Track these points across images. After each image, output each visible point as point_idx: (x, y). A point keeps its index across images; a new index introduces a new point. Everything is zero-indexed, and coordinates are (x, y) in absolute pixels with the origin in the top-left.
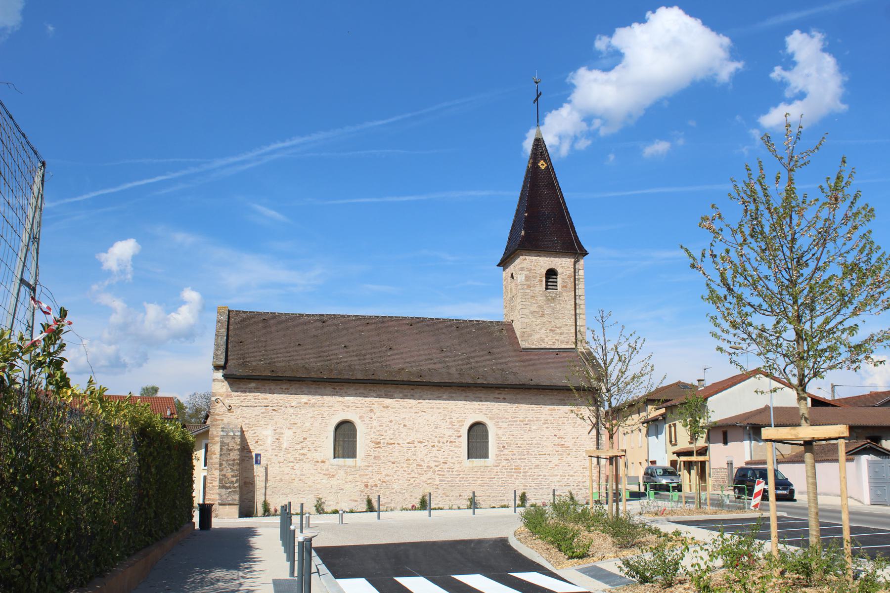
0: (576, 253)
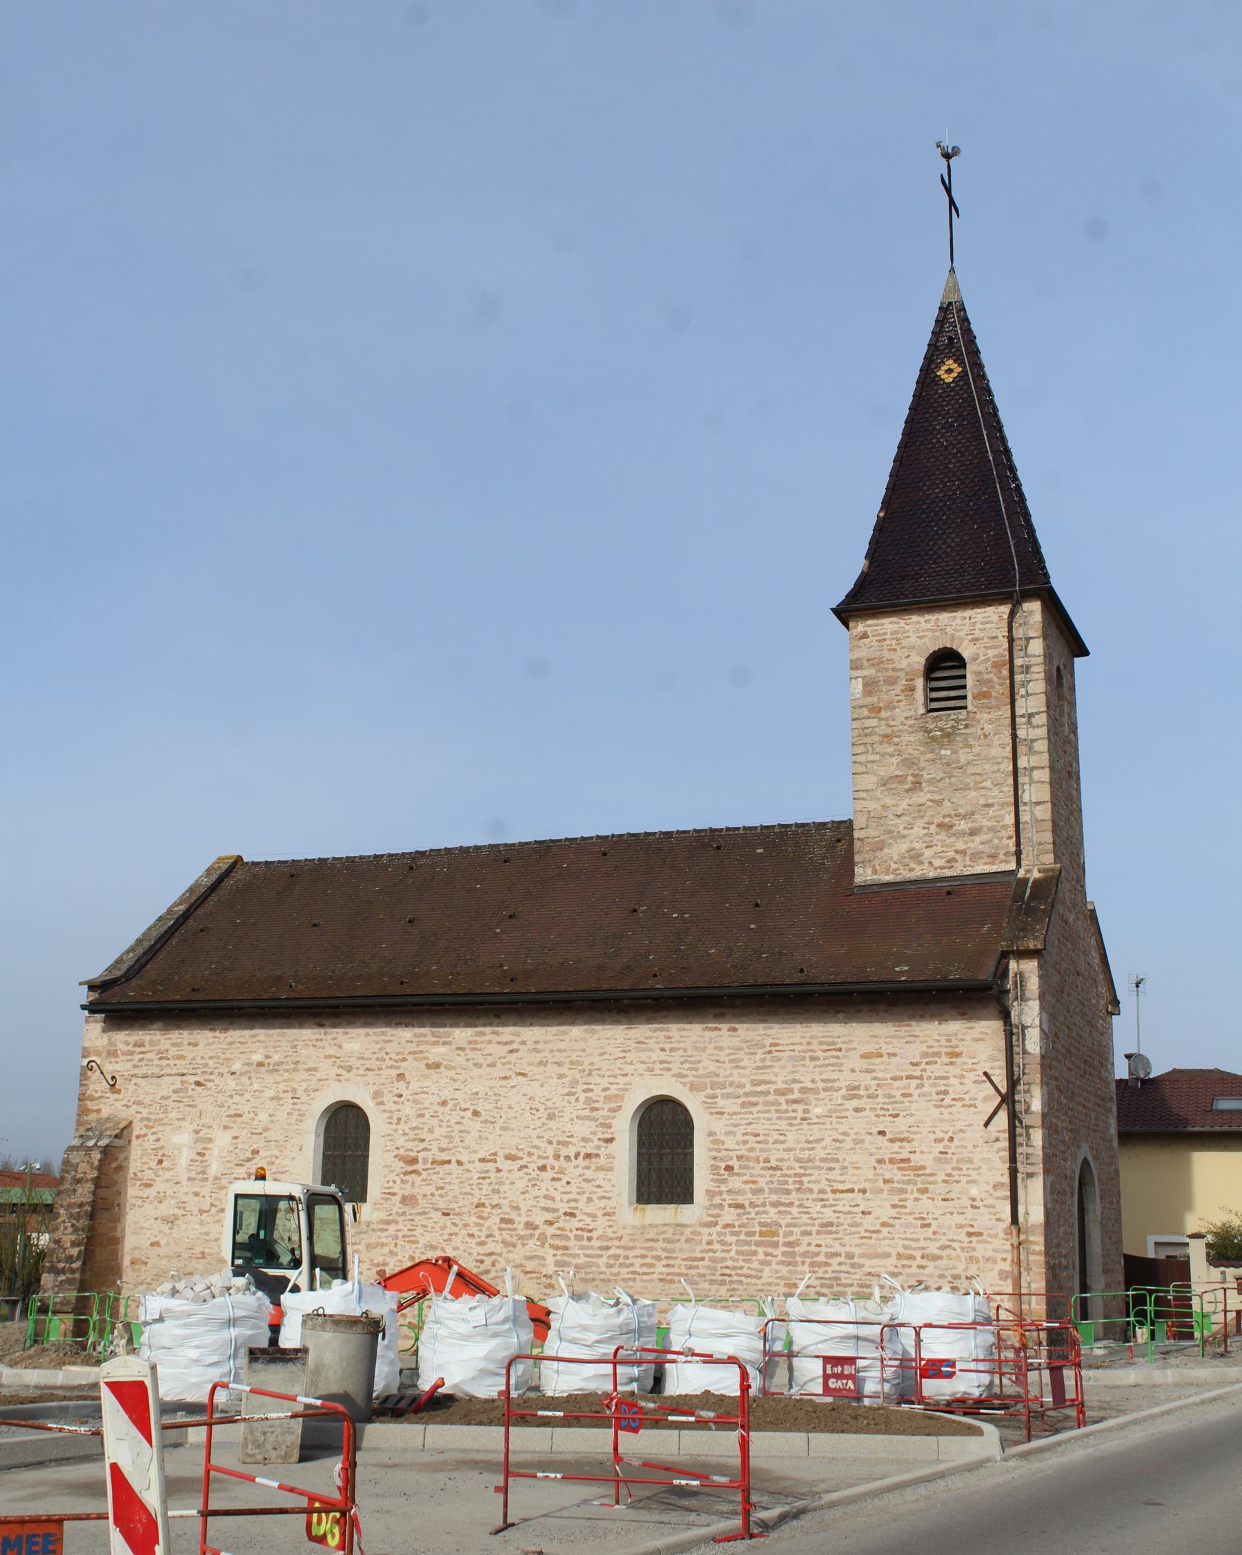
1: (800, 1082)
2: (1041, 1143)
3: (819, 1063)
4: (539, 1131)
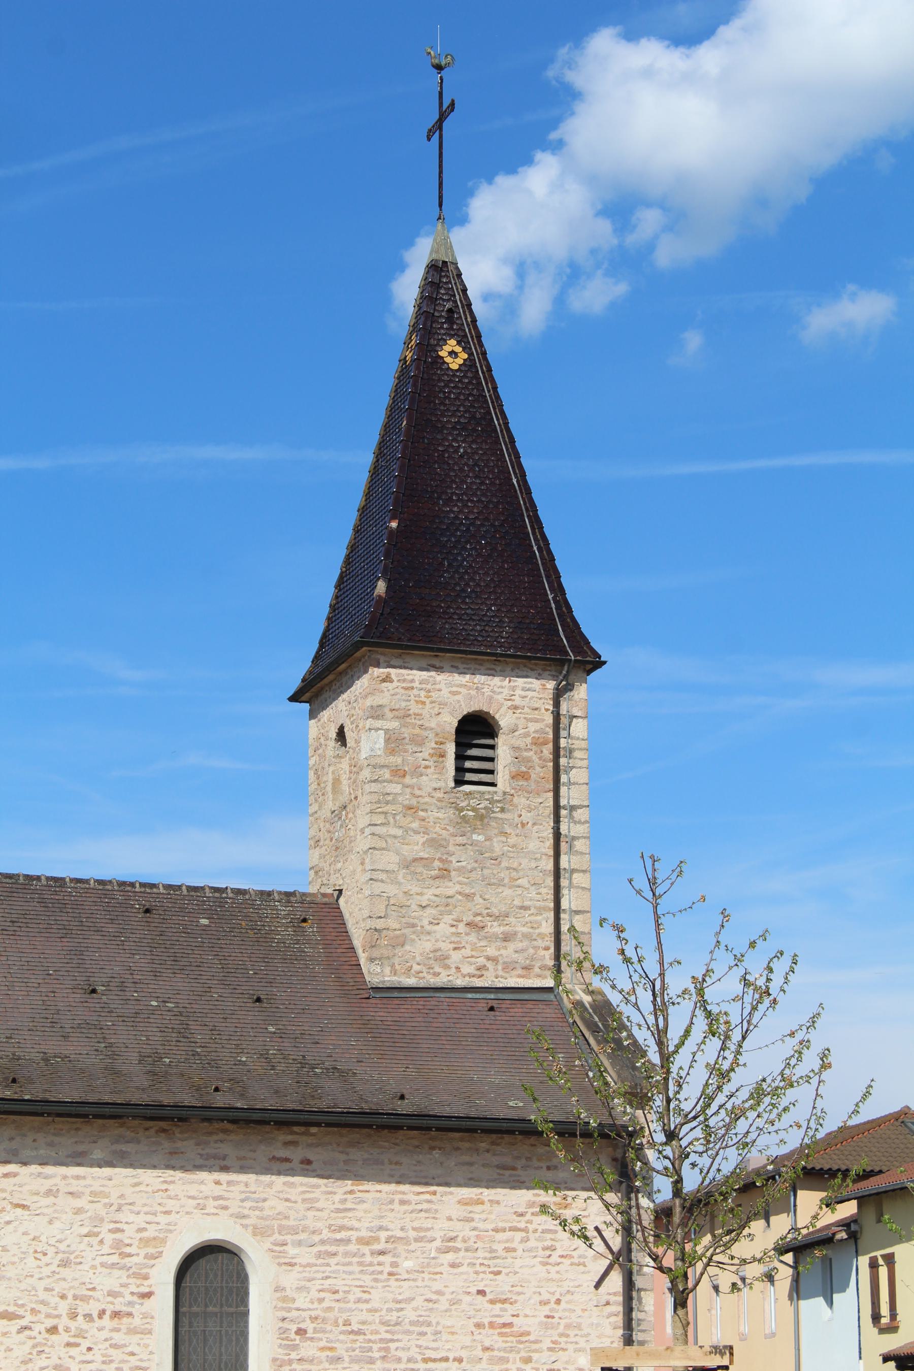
0: (561, 663)
1: (387, 1230)
3: (410, 1208)
4: (46, 1282)
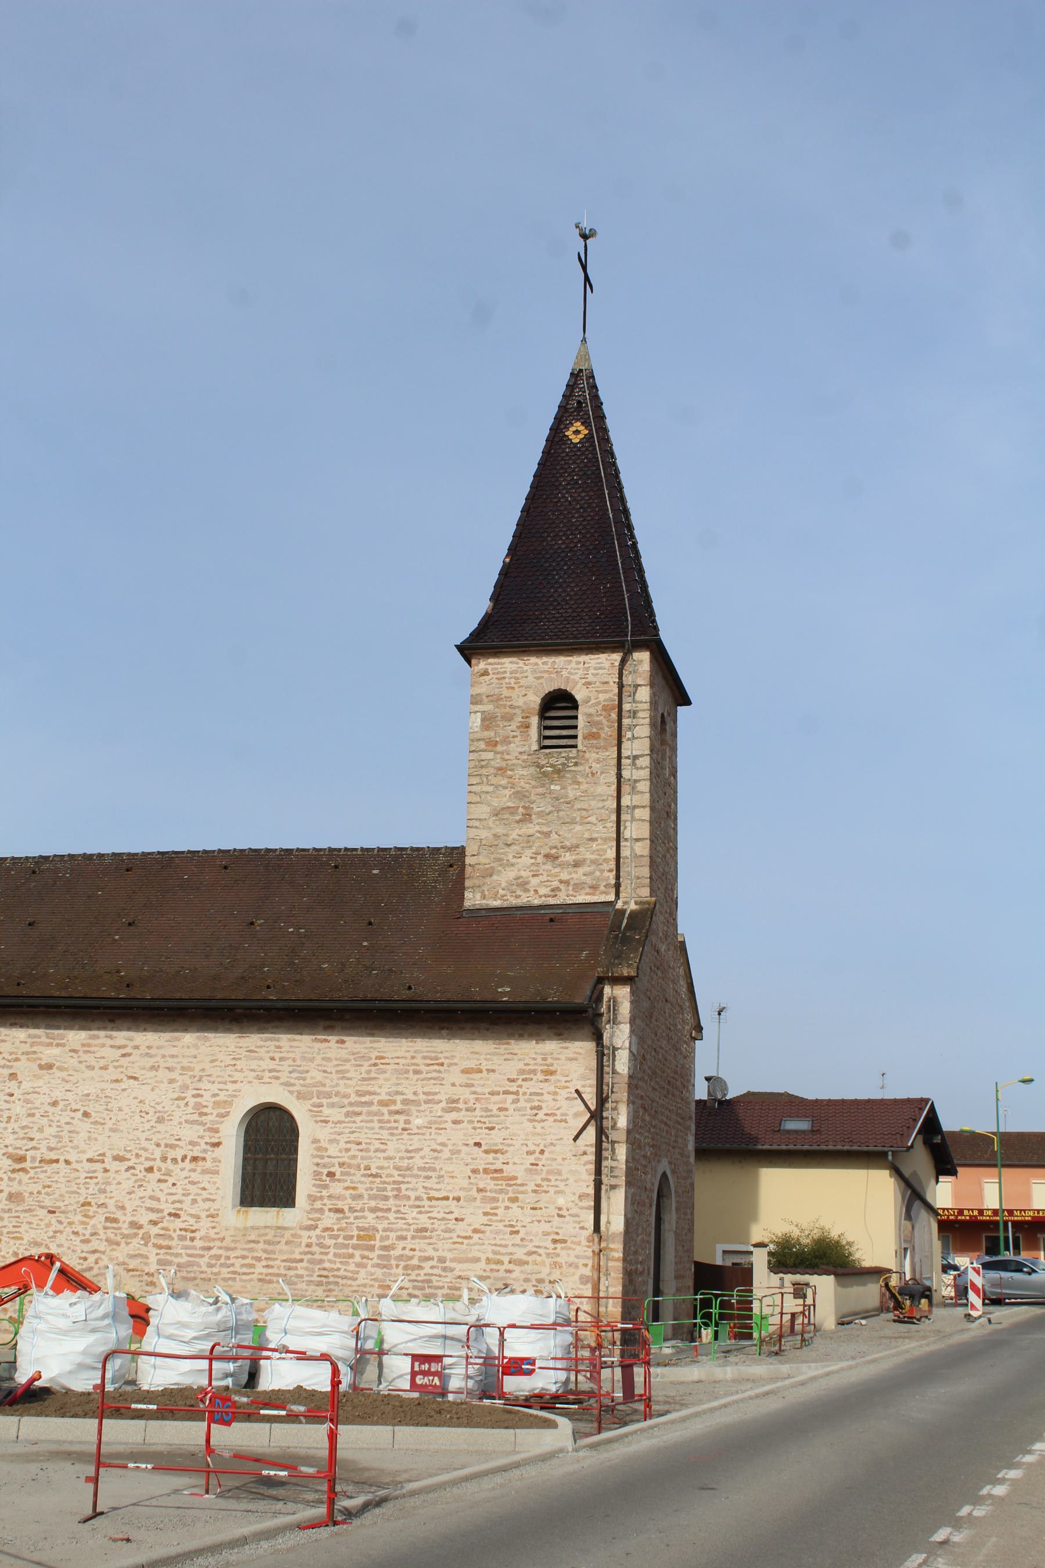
1: (403, 1094)
2: (624, 1158)
3: (422, 1076)
4: (147, 1133)
